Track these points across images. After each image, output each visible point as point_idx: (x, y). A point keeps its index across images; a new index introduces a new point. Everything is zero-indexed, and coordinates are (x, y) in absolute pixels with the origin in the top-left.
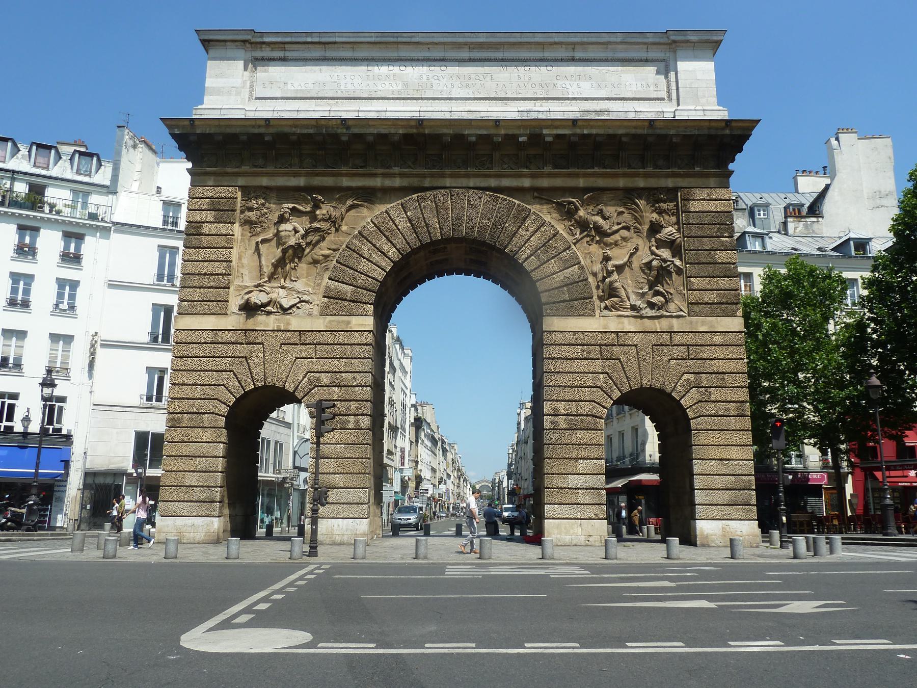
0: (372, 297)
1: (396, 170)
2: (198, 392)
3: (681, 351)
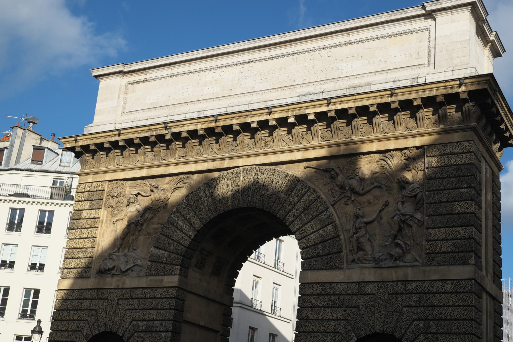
0: (179, 259)
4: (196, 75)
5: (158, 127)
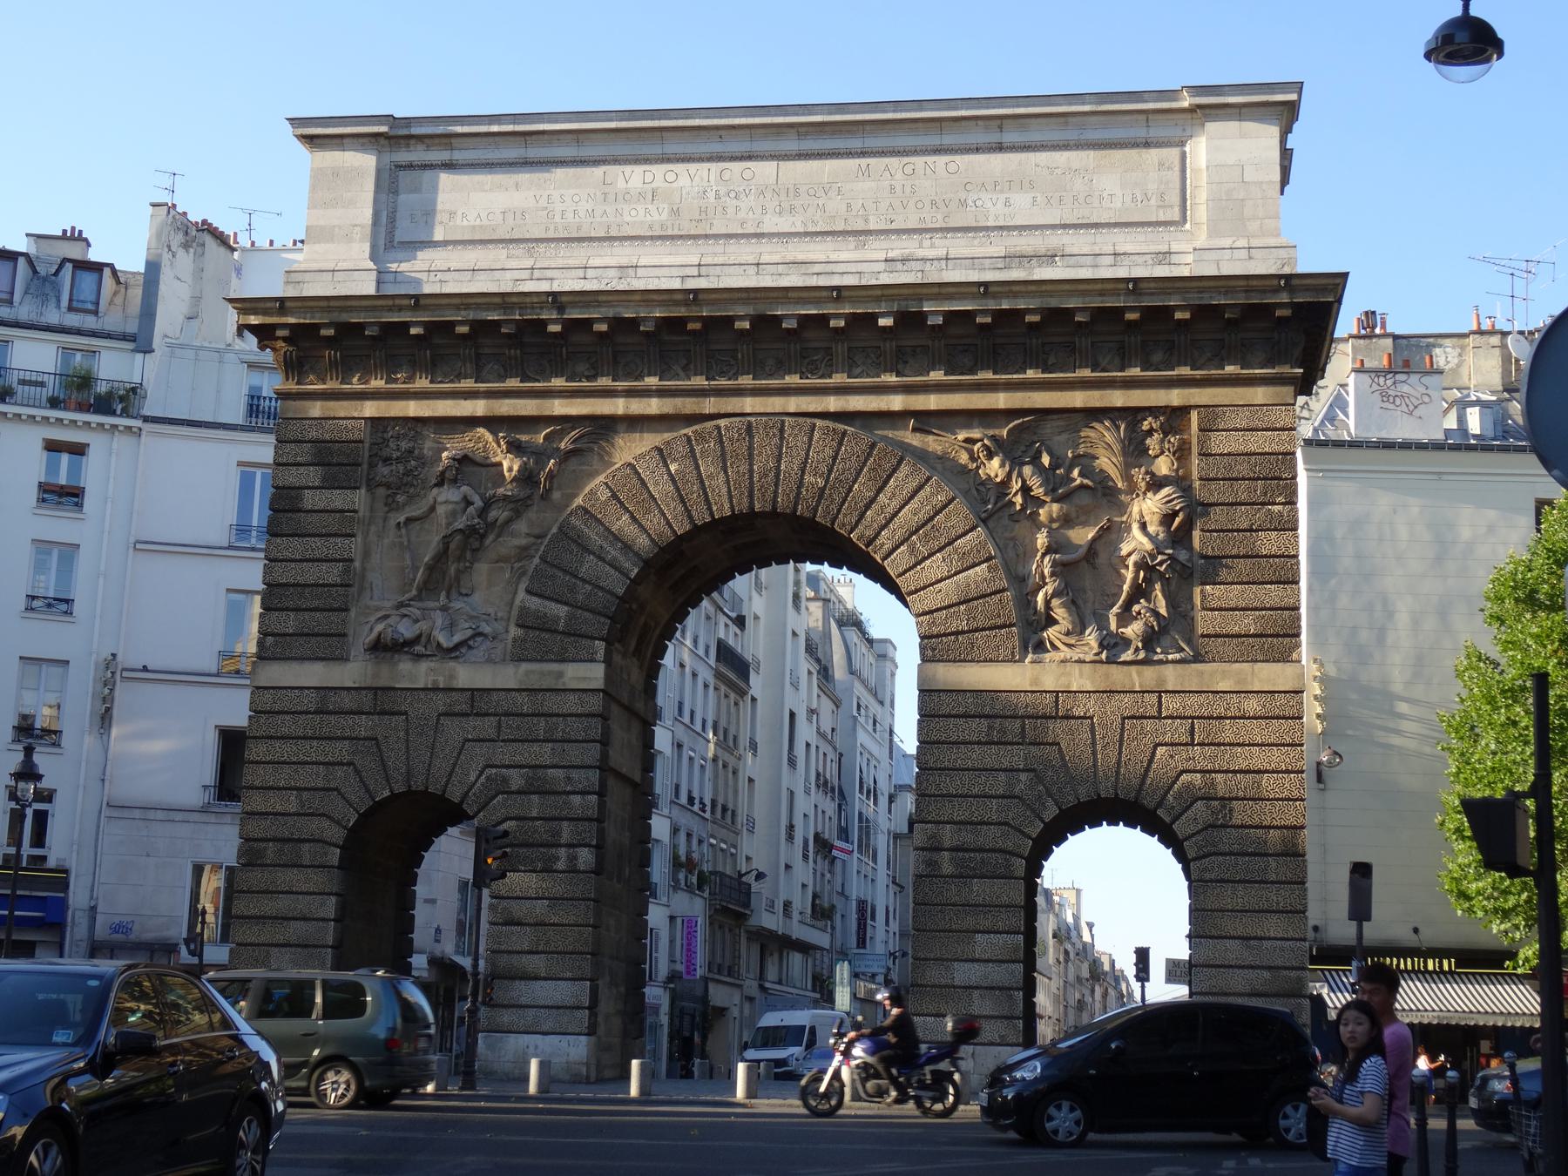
1: (652, 381)
3: (1179, 730)
5: (528, 300)
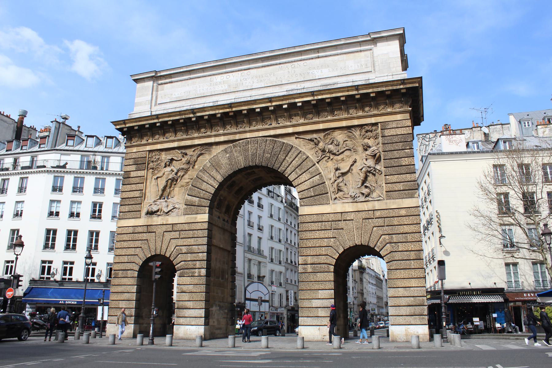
0: (208, 203)
2: (126, 259)
3: (380, 222)
4: (209, 78)
